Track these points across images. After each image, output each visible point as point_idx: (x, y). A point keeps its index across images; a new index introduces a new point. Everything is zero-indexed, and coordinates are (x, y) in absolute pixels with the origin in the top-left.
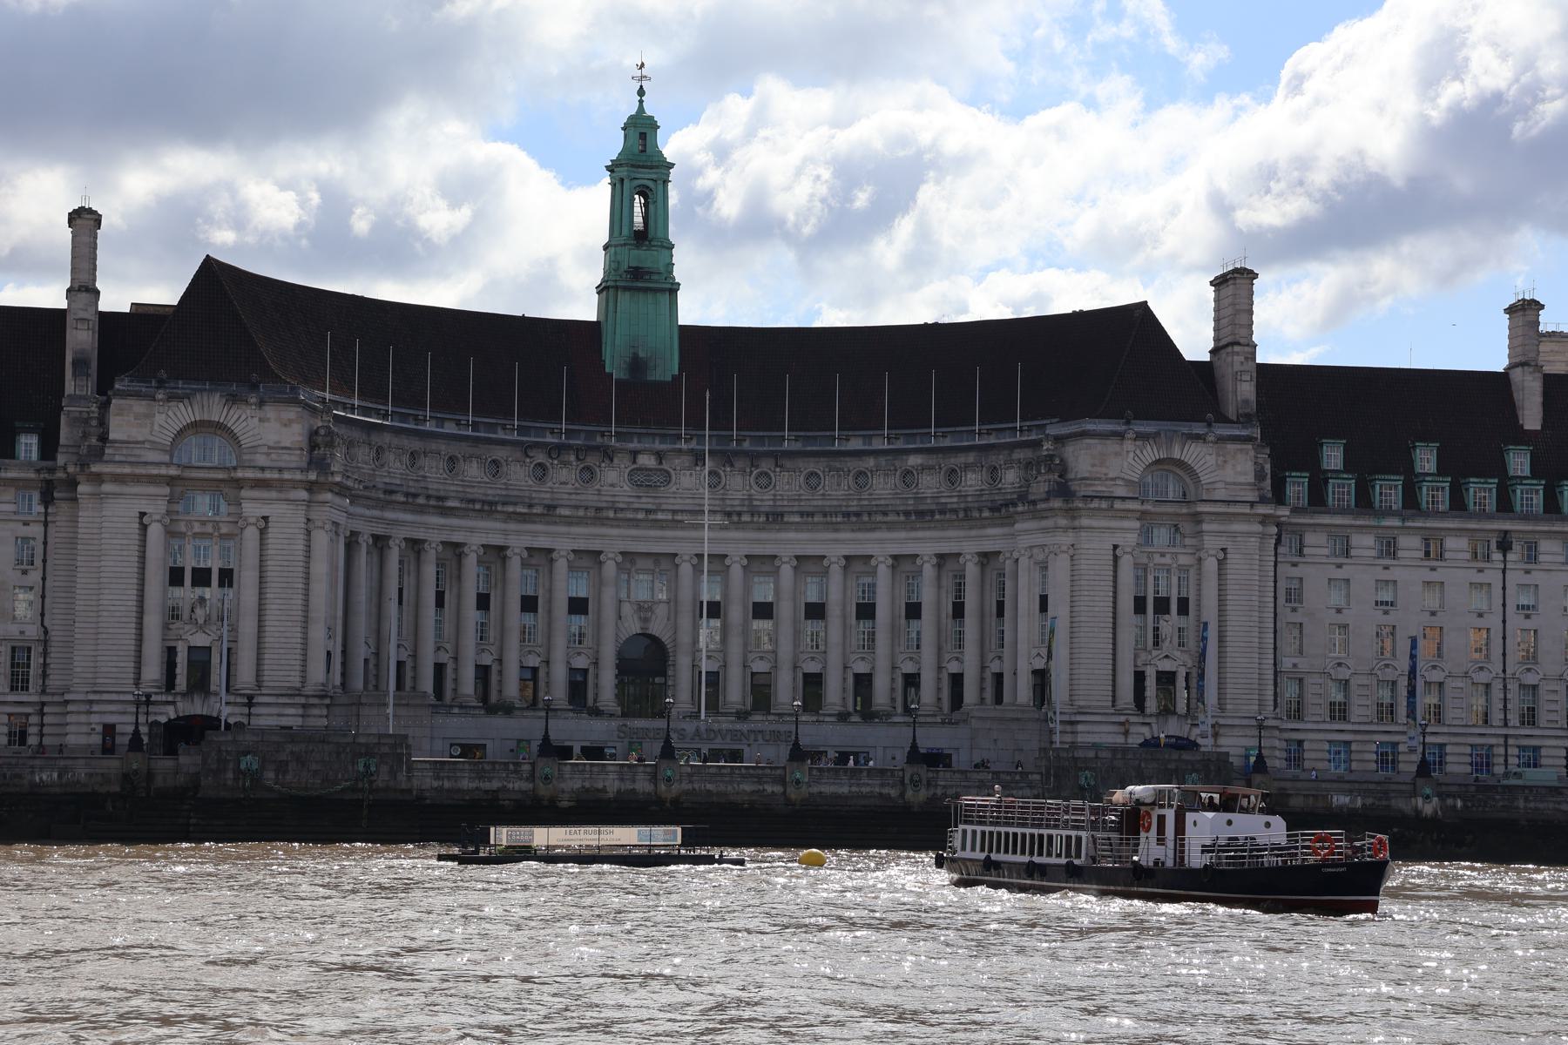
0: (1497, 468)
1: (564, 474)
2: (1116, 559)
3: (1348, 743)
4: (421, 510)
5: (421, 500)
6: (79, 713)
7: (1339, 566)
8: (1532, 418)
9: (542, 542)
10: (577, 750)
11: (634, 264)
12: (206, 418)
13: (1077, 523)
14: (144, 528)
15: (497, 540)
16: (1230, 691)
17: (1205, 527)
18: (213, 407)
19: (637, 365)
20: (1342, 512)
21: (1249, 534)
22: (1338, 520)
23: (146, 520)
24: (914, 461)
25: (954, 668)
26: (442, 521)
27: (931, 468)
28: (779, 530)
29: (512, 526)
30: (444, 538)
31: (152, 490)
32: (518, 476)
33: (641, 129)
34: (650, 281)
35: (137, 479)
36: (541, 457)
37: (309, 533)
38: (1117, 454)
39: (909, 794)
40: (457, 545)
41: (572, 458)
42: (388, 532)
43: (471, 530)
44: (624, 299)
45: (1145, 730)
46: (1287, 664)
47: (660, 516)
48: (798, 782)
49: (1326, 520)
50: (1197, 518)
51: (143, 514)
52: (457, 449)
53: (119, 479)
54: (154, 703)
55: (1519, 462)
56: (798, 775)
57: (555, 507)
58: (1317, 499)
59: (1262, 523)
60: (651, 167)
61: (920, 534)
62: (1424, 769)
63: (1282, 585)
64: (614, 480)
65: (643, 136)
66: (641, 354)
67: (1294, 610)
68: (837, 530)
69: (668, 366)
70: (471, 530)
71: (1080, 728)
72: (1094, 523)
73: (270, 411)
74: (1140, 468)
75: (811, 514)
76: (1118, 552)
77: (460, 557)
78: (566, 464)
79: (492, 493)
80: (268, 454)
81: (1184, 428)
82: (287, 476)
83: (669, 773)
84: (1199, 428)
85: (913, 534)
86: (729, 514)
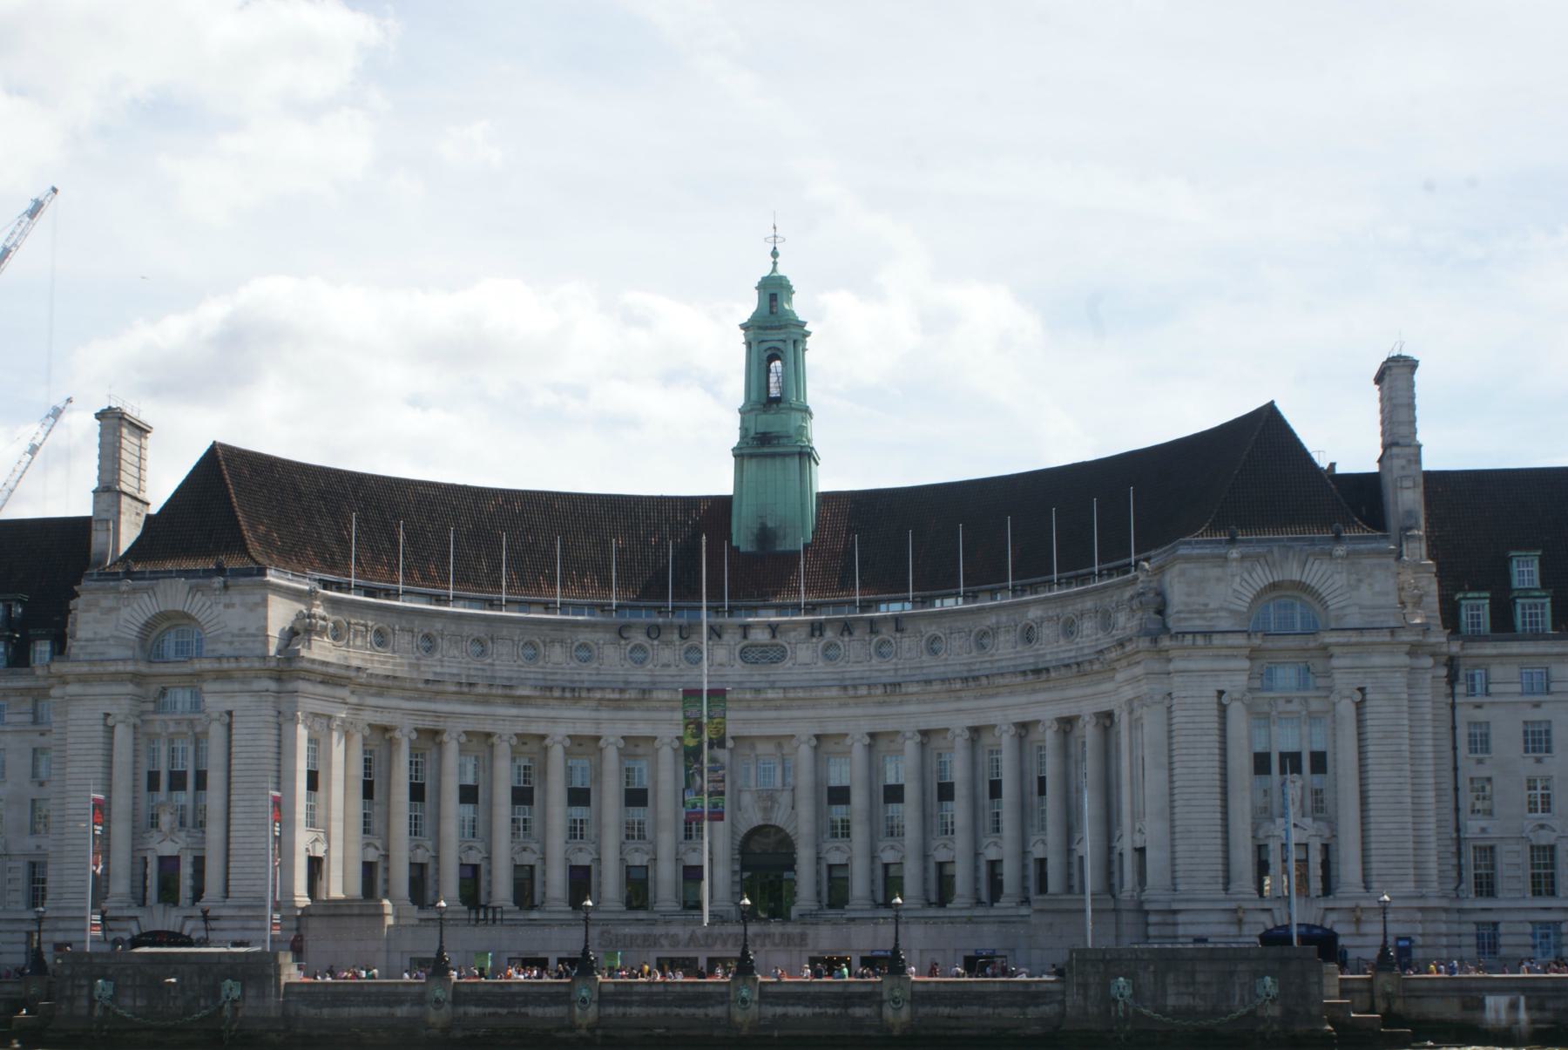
1: (666, 655)
2: (1223, 710)
3: (1557, 924)
4: (485, 700)
5: (480, 690)
6: (234, 929)
7: (1537, 705)
9: (642, 730)
10: (552, 962)
11: (761, 430)
12: (170, 608)
13: (1171, 667)
14: (110, 730)
15: (588, 730)
16: (1375, 865)
17: (1335, 662)
18: (173, 595)
19: (765, 536)
20: (1537, 636)
21: (1392, 668)
22: (1529, 648)
23: (110, 721)
25: (991, 854)
26: (514, 711)
27: (1050, 619)
28: (901, 703)
29: (604, 714)
30: (519, 730)
31: (116, 689)
32: (613, 661)
33: (774, 291)
34: (779, 445)
35: (100, 678)
37: (279, 727)
38: (1219, 580)
39: (888, 1012)
40: (385, 729)
41: (676, 637)
42: (440, 725)
43: (554, 720)
44: (751, 466)
45: (1265, 917)
46: (1473, 826)
47: (770, 695)
48: (744, 1001)
49: (1515, 648)
50: (1326, 652)
51: (107, 715)
53: (83, 679)
54: (217, 918)
56: (745, 993)
57: (650, 691)
58: (1503, 623)
59: (1410, 654)
60: (779, 328)
61: (1041, 696)
63: (1462, 732)
65: (773, 298)
66: (770, 524)
67: (1480, 762)
68: (959, 699)
70: (554, 720)
71: (1181, 918)
72: (1192, 665)
74: (1249, 595)
75: (928, 682)
76: (1225, 700)
77: (391, 743)
78: (668, 644)
80: (231, 643)
82: (245, 665)
83: (584, 993)
85: (1034, 698)
86: (845, 688)
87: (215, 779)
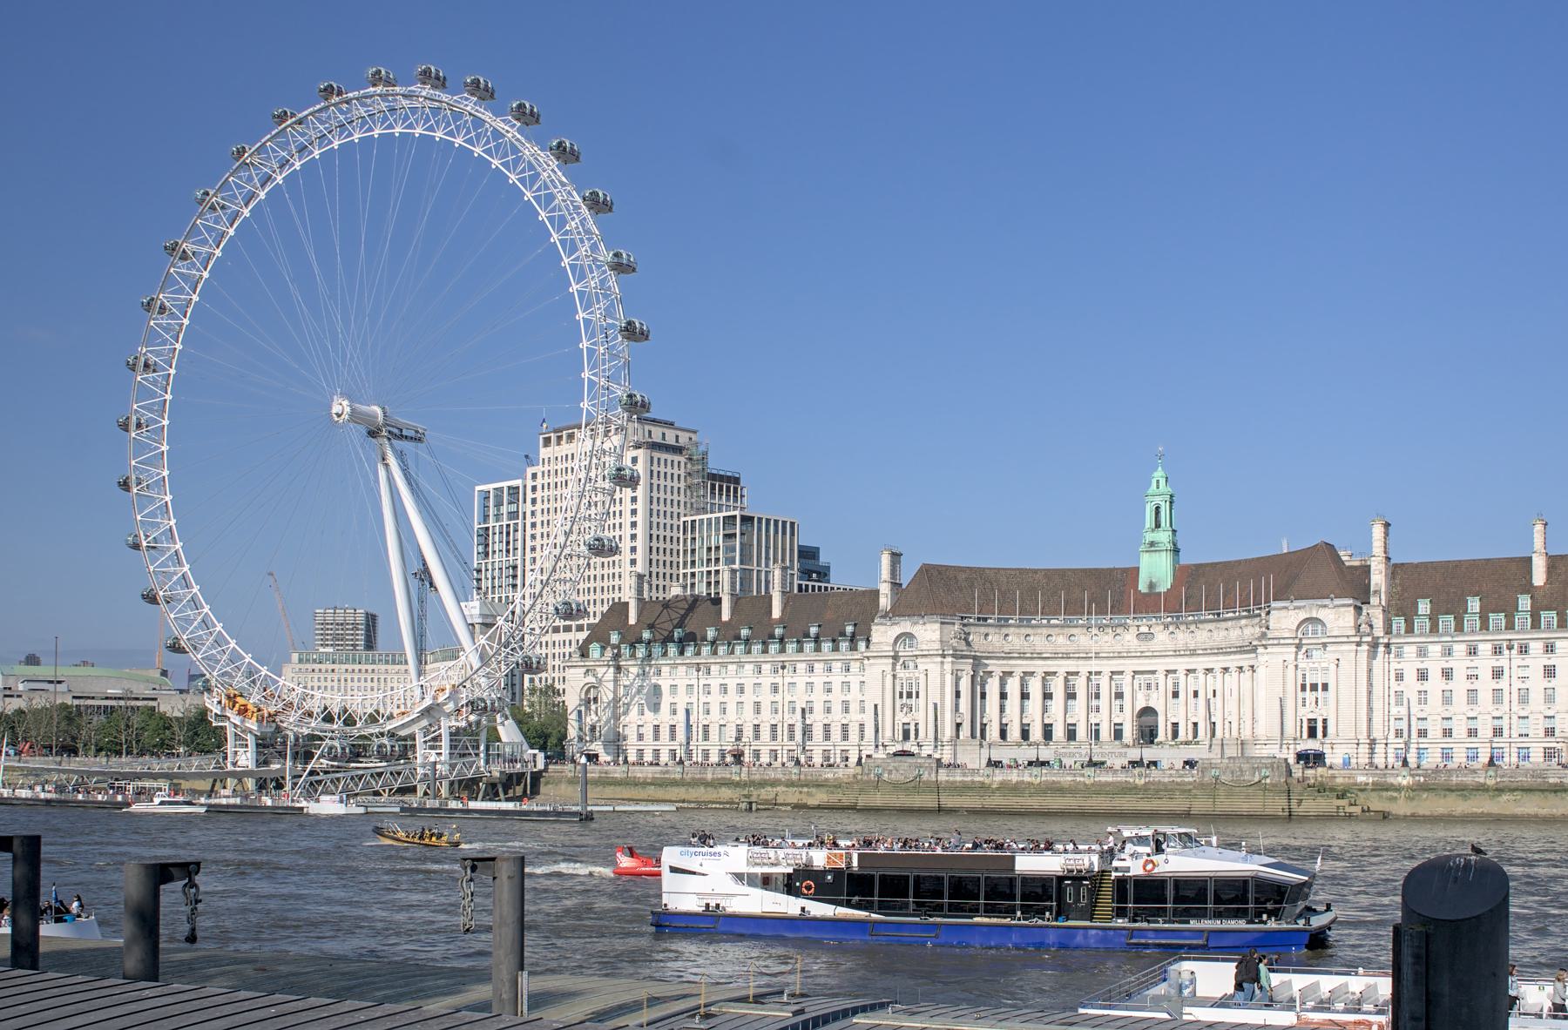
0: (1510, 611)
1: (1106, 638)
8: (1539, 577)
19: (1152, 586)
24: (1243, 622)
36: (1094, 631)
52: (1050, 631)
55: (1525, 602)
62: (1491, 763)
64: (1129, 639)
69: (1165, 585)
73: (928, 626)
79: (1071, 649)
81: (1319, 602)
84: (1326, 602)
87: (922, 694)
